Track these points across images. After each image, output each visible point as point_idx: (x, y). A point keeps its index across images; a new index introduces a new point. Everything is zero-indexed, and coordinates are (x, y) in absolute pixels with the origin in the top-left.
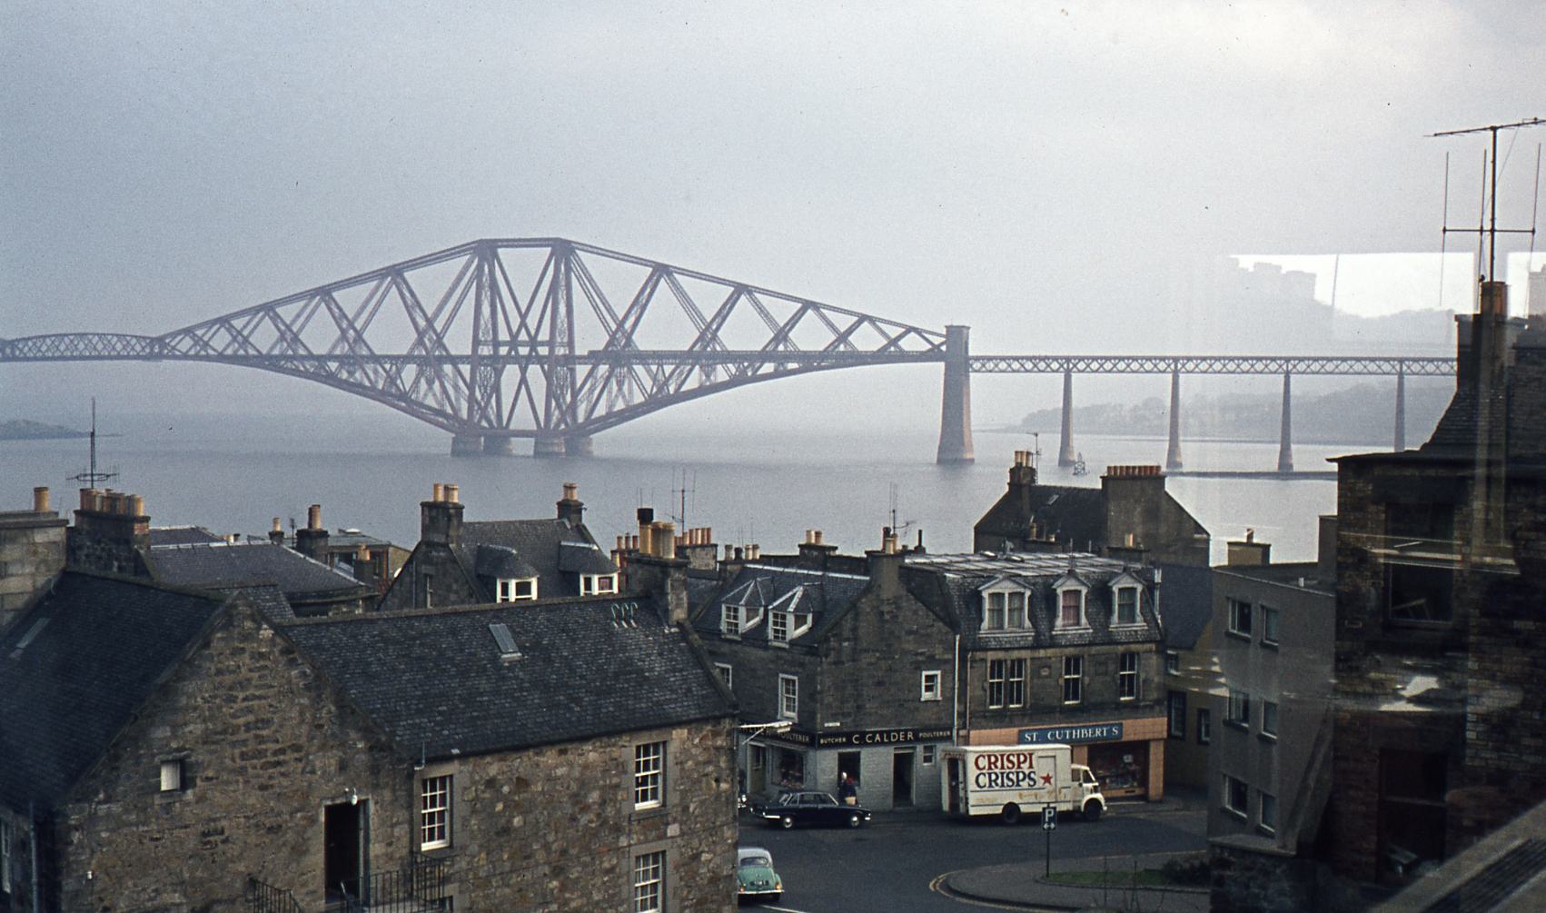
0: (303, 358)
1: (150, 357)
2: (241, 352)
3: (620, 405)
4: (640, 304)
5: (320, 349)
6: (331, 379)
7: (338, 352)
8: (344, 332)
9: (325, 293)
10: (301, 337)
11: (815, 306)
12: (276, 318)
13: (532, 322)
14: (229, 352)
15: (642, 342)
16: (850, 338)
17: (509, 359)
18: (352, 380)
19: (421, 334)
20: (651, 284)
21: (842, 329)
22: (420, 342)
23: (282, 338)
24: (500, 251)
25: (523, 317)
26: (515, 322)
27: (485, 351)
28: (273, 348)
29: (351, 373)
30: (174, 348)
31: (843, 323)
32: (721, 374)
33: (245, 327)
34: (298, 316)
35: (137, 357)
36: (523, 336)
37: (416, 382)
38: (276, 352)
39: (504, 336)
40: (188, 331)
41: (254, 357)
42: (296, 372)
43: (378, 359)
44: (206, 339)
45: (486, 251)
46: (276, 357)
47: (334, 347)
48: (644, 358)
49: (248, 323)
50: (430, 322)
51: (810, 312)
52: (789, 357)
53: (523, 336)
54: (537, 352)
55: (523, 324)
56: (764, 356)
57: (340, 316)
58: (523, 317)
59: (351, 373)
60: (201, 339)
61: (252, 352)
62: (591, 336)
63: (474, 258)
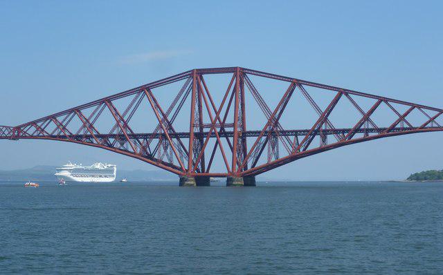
1: (15, 138)
2: (62, 134)
3: (273, 160)
6: (110, 147)
7: (115, 132)
8: (118, 122)
9: (107, 101)
10: (94, 126)
11: (386, 100)
12: (81, 116)
13: (222, 116)
14: (56, 134)
15: (286, 123)
16: (372, 117)
17: (213, 135)
18: (122, 148)
20: (290, 93)
21: (402, 114)
24: (205, 76)
25: (217, 113)
26: (214, 115)
27: (197, 130)
28: (79, 131)
29: (122, 144)
30: (25, 132)
31: (402, 109)
32: (332, 139)
33: (64, 120)
34: (93, 114)
35: (6, 138)
36: (218, 122)
37: (156, 149)
39: (206, 120)
40: (33, 123)
41: (70, 136)
42: (91, 144)
43: (136, 137)
44: (43, 127)
45: (197, 76)
46: (81, 136)
47: (113, 130)
48: (285, 133)
49: (66, 118)
50: (165, 116)
51: (383, 103)
52: (371, 130)
53: (218, 122)
54: (224, 131)
55: (218, 118)
56: (357, 130)
57: (115, 112)
58: (217, 113)
59: (122, 144)
60: (40, 127)
61: (67, 134)
62: (256, 120)
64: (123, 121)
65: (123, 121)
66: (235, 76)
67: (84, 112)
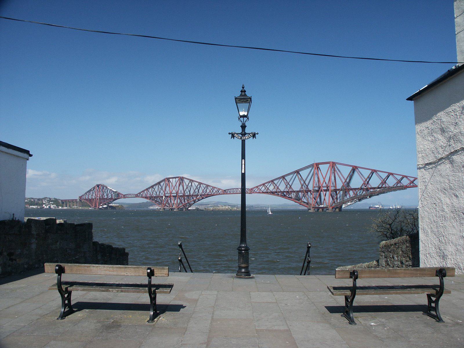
0: (279, 192)
4: (351, 177)
5: (282, 190)
6: (284, 196)
7: (285, 190)
8: (287, 186)
11: (392, 174)
15: (353, 185)
19: (302, 185)
22: (302, 188)
23: (274, 188)
27: (317, 189)
30: (254, 191)
31: (399, 177)
33: (267, 186)
34: (278, 183)
38: (273, 191)
41: (269, 192)
43: (294, 192)
46: (273, 192)
47: (285, 189)
48: (352, 189)
50: (305, 182)
53: (324, 185)
59: (289, 195)
63: (313, 168)
64: (289, 185)
65: (289, 185)
66: (330, 165)
67: (276, 182)
